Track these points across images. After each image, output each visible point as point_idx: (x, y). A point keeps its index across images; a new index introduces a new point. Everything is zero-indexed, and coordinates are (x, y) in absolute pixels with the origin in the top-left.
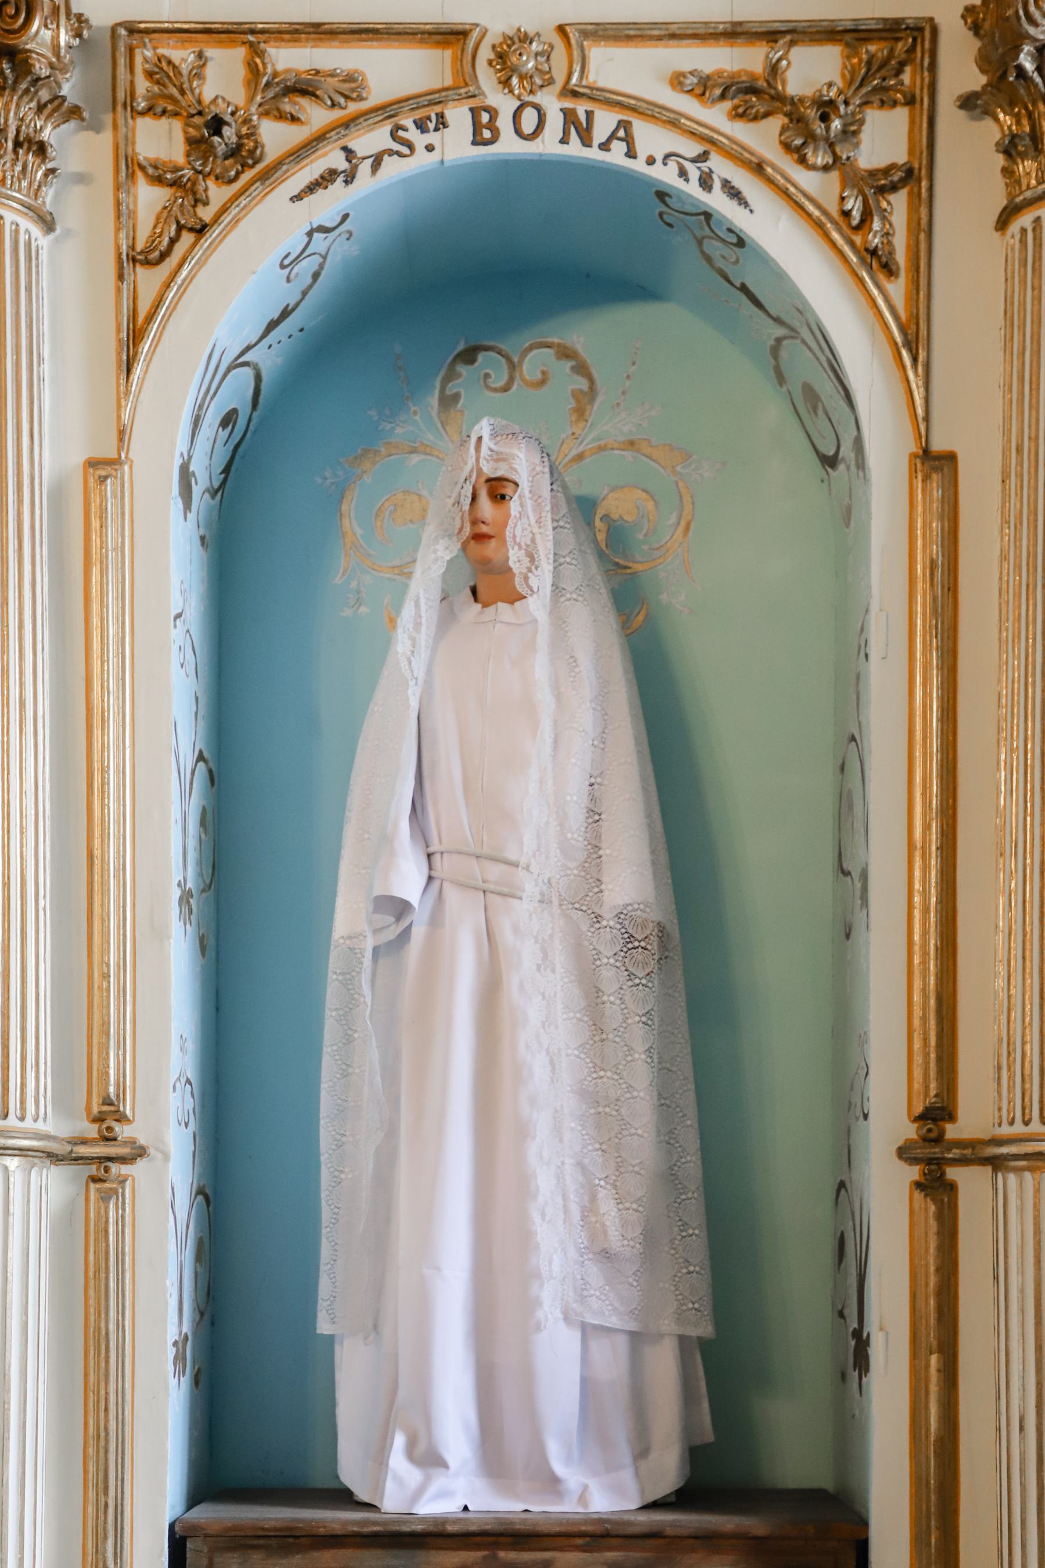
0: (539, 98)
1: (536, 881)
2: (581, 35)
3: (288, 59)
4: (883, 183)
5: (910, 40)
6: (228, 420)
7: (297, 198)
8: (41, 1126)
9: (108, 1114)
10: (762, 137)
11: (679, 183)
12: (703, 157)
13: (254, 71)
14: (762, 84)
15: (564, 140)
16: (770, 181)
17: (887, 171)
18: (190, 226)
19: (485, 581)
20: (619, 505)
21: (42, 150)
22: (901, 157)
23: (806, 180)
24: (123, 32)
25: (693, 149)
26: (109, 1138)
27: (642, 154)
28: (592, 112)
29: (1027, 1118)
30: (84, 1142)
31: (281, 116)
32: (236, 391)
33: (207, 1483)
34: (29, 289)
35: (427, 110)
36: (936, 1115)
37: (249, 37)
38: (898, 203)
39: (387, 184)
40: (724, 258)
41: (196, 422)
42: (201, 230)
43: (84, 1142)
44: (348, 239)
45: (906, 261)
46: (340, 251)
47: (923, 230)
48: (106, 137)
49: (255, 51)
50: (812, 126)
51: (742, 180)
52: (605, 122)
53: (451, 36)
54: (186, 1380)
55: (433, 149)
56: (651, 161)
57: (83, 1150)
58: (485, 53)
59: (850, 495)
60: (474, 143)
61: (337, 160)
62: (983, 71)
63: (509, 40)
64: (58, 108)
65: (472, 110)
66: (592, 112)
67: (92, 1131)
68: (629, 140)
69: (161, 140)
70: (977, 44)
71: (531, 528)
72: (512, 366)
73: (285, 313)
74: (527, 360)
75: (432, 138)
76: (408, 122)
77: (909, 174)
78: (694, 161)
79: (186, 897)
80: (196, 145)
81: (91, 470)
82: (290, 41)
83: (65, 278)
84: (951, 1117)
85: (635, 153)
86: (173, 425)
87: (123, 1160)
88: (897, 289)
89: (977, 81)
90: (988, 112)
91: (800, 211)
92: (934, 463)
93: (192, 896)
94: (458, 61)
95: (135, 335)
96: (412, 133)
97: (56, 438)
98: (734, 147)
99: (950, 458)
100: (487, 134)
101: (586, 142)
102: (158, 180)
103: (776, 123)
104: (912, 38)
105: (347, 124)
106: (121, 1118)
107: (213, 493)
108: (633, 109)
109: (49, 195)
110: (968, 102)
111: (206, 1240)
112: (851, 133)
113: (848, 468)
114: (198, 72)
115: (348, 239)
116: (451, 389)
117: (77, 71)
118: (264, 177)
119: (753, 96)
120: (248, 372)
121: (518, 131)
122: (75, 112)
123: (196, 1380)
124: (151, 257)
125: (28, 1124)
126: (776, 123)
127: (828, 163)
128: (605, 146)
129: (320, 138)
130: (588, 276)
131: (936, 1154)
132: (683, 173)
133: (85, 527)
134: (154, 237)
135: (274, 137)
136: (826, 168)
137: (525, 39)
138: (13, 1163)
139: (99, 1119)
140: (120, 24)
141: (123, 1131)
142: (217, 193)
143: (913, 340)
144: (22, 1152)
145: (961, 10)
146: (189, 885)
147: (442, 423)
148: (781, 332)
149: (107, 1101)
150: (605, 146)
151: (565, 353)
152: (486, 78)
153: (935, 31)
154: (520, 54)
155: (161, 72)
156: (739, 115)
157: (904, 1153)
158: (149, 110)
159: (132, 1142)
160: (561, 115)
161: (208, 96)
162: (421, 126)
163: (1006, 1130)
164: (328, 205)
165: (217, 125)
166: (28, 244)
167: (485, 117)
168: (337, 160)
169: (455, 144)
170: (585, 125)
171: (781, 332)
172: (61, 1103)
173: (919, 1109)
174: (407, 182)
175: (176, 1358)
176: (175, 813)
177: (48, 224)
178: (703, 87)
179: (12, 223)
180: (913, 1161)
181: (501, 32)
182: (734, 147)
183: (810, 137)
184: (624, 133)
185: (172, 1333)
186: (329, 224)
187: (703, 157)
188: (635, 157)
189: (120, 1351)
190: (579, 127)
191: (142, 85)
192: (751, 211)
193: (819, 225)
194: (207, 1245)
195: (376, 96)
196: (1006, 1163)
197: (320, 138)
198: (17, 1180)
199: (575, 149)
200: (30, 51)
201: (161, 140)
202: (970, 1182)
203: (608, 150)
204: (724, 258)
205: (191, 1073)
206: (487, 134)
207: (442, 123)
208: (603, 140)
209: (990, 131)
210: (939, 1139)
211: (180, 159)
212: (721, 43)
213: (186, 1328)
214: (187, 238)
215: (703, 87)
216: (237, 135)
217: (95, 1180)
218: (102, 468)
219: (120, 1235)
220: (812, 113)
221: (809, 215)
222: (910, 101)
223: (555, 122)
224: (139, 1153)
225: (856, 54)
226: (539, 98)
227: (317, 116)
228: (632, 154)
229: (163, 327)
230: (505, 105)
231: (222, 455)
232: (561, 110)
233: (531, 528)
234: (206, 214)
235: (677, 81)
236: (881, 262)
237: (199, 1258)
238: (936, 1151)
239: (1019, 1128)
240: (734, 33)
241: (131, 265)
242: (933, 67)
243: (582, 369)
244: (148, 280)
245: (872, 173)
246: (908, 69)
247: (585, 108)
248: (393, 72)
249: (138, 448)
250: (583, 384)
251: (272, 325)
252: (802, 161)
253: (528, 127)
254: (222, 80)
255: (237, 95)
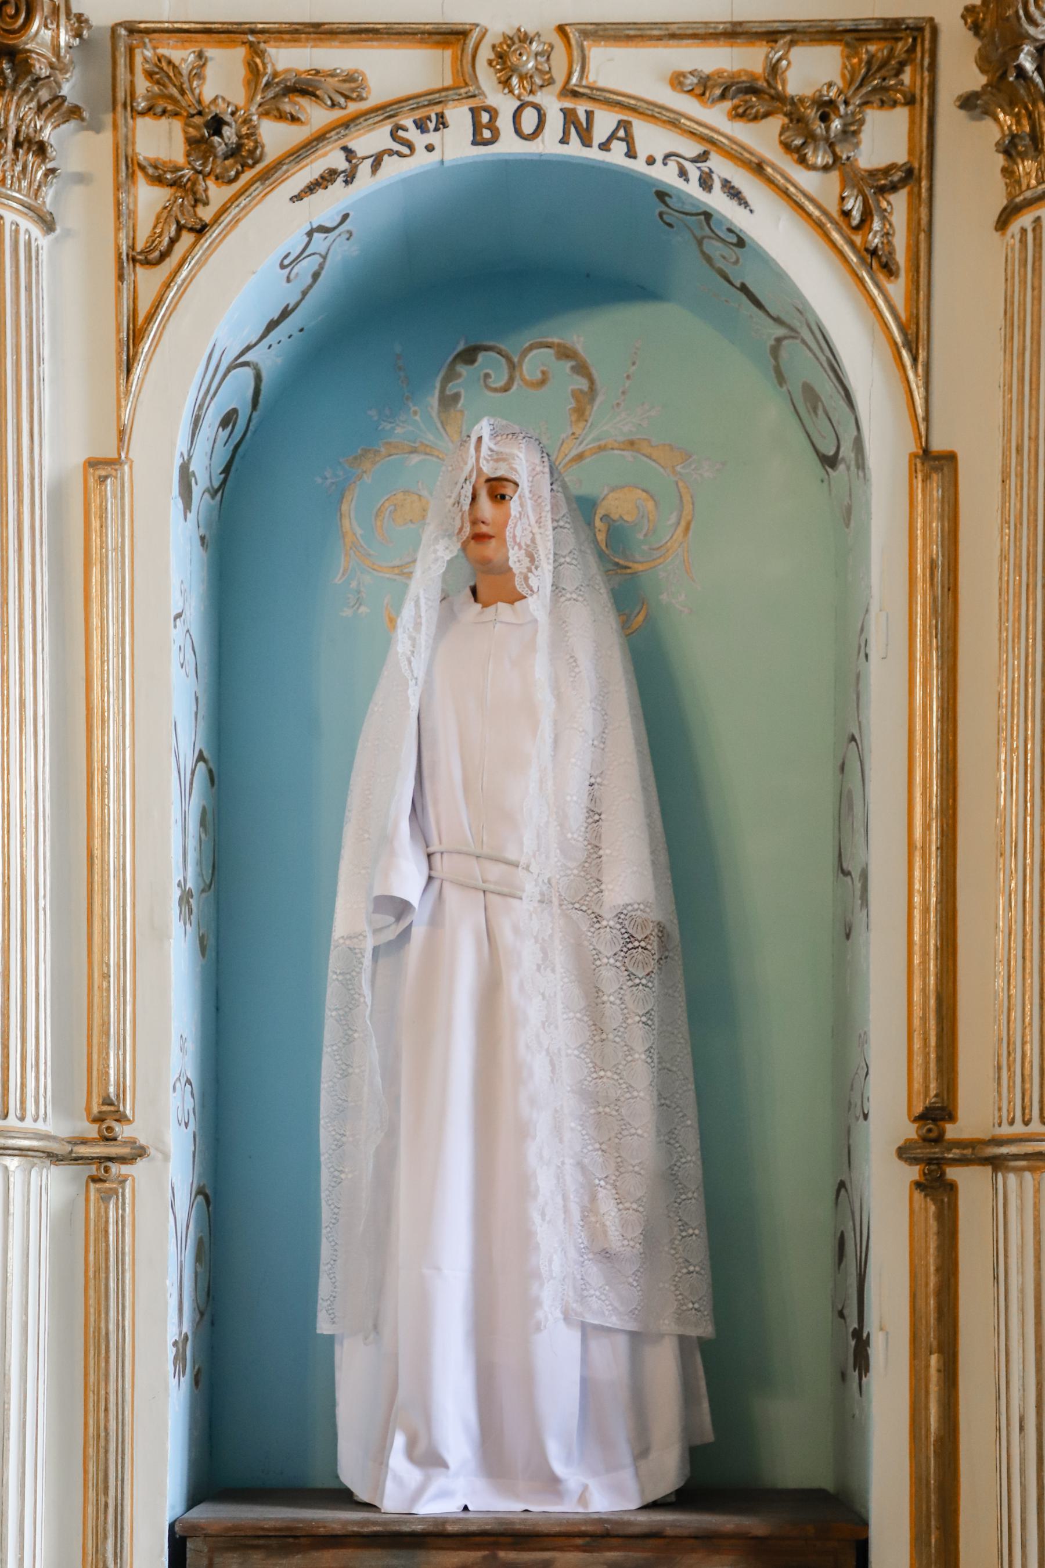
0: (539, 98)
1: (536, 881)
2: (581, 35)
3: (288, 59)
4: (883, 183)
5: (910, 40)
6: (228, 420)
7: (297, 198)
8: (41, 1126)
9: (108, 1114)
10: (762, 137)
11: (679, 183)
12: (704, 157)
13: (254, 71)
14: (762, 84)
15: (564, 140)
16: (770, 181)
17: (887, 171)
18: (190, 226)
19: (485, 581)
20: (619, 505)
21: (41, 150)
22: (901, 157)
23: (806, 180)
24: (123, 32)
25: (693, 149)
26: (109, 1138)
27: (642, 154)
28: (592, 112)
29: (1027, 1118)
30: (84, 1142)
31: (281, 116)
32: (236, 391)
33: (207, 1483)
34: (29, 289)
35: (427, 110)
36: (936, 1115)
37: (249, 37)
38: (898, 203)
39: (387, 184)
40: (724, 258)
41: (196, 422)
42: (201, 230)
43: (84, 1142)
44: (348, 239)
45: (906, 261)
46: (340, 251)
47: (923, 230)
48: (106, 138)
49: (255, 51)
50: (812, 126)
51: (742, 180)
52: (605, 122)
53: (451, 36)
54: (186, 1380)
55: (433, 149)
56: (651, 161)
57: (83, 1150)
58: (485, 53)
59: (850, 495)
60: (474, 143)
61: (337, 160)
62: (983, 71)
63: (509, 40)
64: (58, 108)
65: (472, 110)
66: (592, 112)
67: (92, 1131)
68: (629, 140)
69: (161, 140)
70: (977, 44)
71: (531, 528)
72: (512, 366)
73: (285, 313)
74: (527, 360)
75: (432, 138)
76: (408, 122)
77: (909, 174)
78: (694, 161)
79: (186, 897)
80: (196, 145)
81: (91, 470)
82: (290, 41)
83: (65, 278)
84: (951, 1117)
85: (635, 153)
86: (173, 425)
87: (123, 1160)
88: (897, 289)
89: (977, 81)
90: (988, 112)
91: (800, 211)
92: (934, 463)
93: (192, 896)
94: (458, 61)
95: (135, 335)
96: (412, 134)
97: (56, 438)
98: (734, 147)
99: (950, 458)
100: (487, 134)
101: (586, 142)
102: (158, 180)
103: (776, 123)
104: (912, 38)
105: (347, 124)
106: (121, 1118)
107: (213, 493)
108: (633, 109)
109: (49, 195)
110: (968, 102)
111: (206, 1240)
112: (851, 133)
113: (848, 468)
114: (198, 73)
115: (348, 239)
116: (451, 389)
117: (77, 71)
118: (264, 177)
119: (753, 96)
120: (248, 372)
121: (518, 131)
122: (75, 112)
123: (196, 1380)
124: (151, 257)
125: (28, 1124)
126: (776, 123)
127: (828, 163)
128: (605, 146)
129: (320, 138)
130: (588, 276)
131: (936, 1154)
132: (683, 173)
133: (85, 527)
134: (154, 237)
135: (274, 137)
136: (826, 168)
137: (525, 39)
138: (13, 1163)
139: (99, 1119)
140: (120, 24)
141: (123, 1131)
142: (217, 193)
143: (913, 340)
144: (22, 1152)
145: (961, 10)
146: (189, 885)
147: (442, 423)
148: (781, 332)
149: (107, 1101)
150: (605, 146)
151: (565, 353)
152: (486, 78)
153: (935, 31)
154: (520, 54)
155: (161, 72)
156: (739, 115)
157: (904, 1153)
158: (149, 110)
159: (132, 1142)
160: (561, 115)
161: (207, 96)
162: (421, 126)
163: (1006, 1130)
164: (328, 205)
165: (217, 125)
166: (28, 244)
167: (485, 117)
168: (337, 160)
169: (455, 144)
170: (585, 125)
171: (781, 332)
172: (61, 1103)
173: (919, 1109)
174: (408, 182)
175: (176, 1358)
176: (175, 813)
177: (48, 224)
178: (703, 87)
179: (12, 223)
180: (913, 1161)
181: (501, 32)
182: (734, 147)
183: (810, 137)
184: (624, 133)
185: (172, 1333)
186: (329, 224)
187: (704, 157)
188: (635, 157)
189: (120, 1351)
190: (579, 127)
191: (142, 85)
192: (751, 211)
193: (819, 225)
194: (207, 1245)
195: (376, 96)
196: (1007, 1163)
197: (320, 138)
198: (17, 1180)
199: (575, 149)
200: (30, 51)
201: (161, 140)
202: (971, 1182)
203: (608, 150)
204: (724, 258)
205: (191, 1073)
206: (487, 134)
207: (442, 123)
208: (603, 140)
209: (990, 131)
210: (939, 1139)
211: (180, 159)
212: (721, 43)
213: (186, 1328)
214: (187, 238)
215: (703, 87)
216: (237, 135)
217: (95, 1180)
218: (102, 468)
219: (120, 1235)
220: (812, 113)
221: (809, 215)
222: (910, 101)
223: (555, 122)
224: (139, 1153)
225: (857, 54)
226: (539, 98)
227: (317, 116)
228: (631, 154)
229: (163, 327)
230: (505, 105)
231: (222, 455)
232: (561, 110)
233: (531, 528)
234: (206, 214)
235: (677, 81)
236: (881, 262)
237: (199, 1258)
238: (936, 1151)
239: (1019, 1128)
240: (734, 33)
241: (131, 265)
242: (933, 67)
243: (582, 369)
244: (148, 280)
245: (872, 173)
246: (908, 69)
247: (585, 108)
248: (393, 72)
249: (138, 448)
250: (583, 384)
251: (272, 325)
252: (802, 161)
253: (528, 127)
254: (222, 80)
255: (237, 95)
